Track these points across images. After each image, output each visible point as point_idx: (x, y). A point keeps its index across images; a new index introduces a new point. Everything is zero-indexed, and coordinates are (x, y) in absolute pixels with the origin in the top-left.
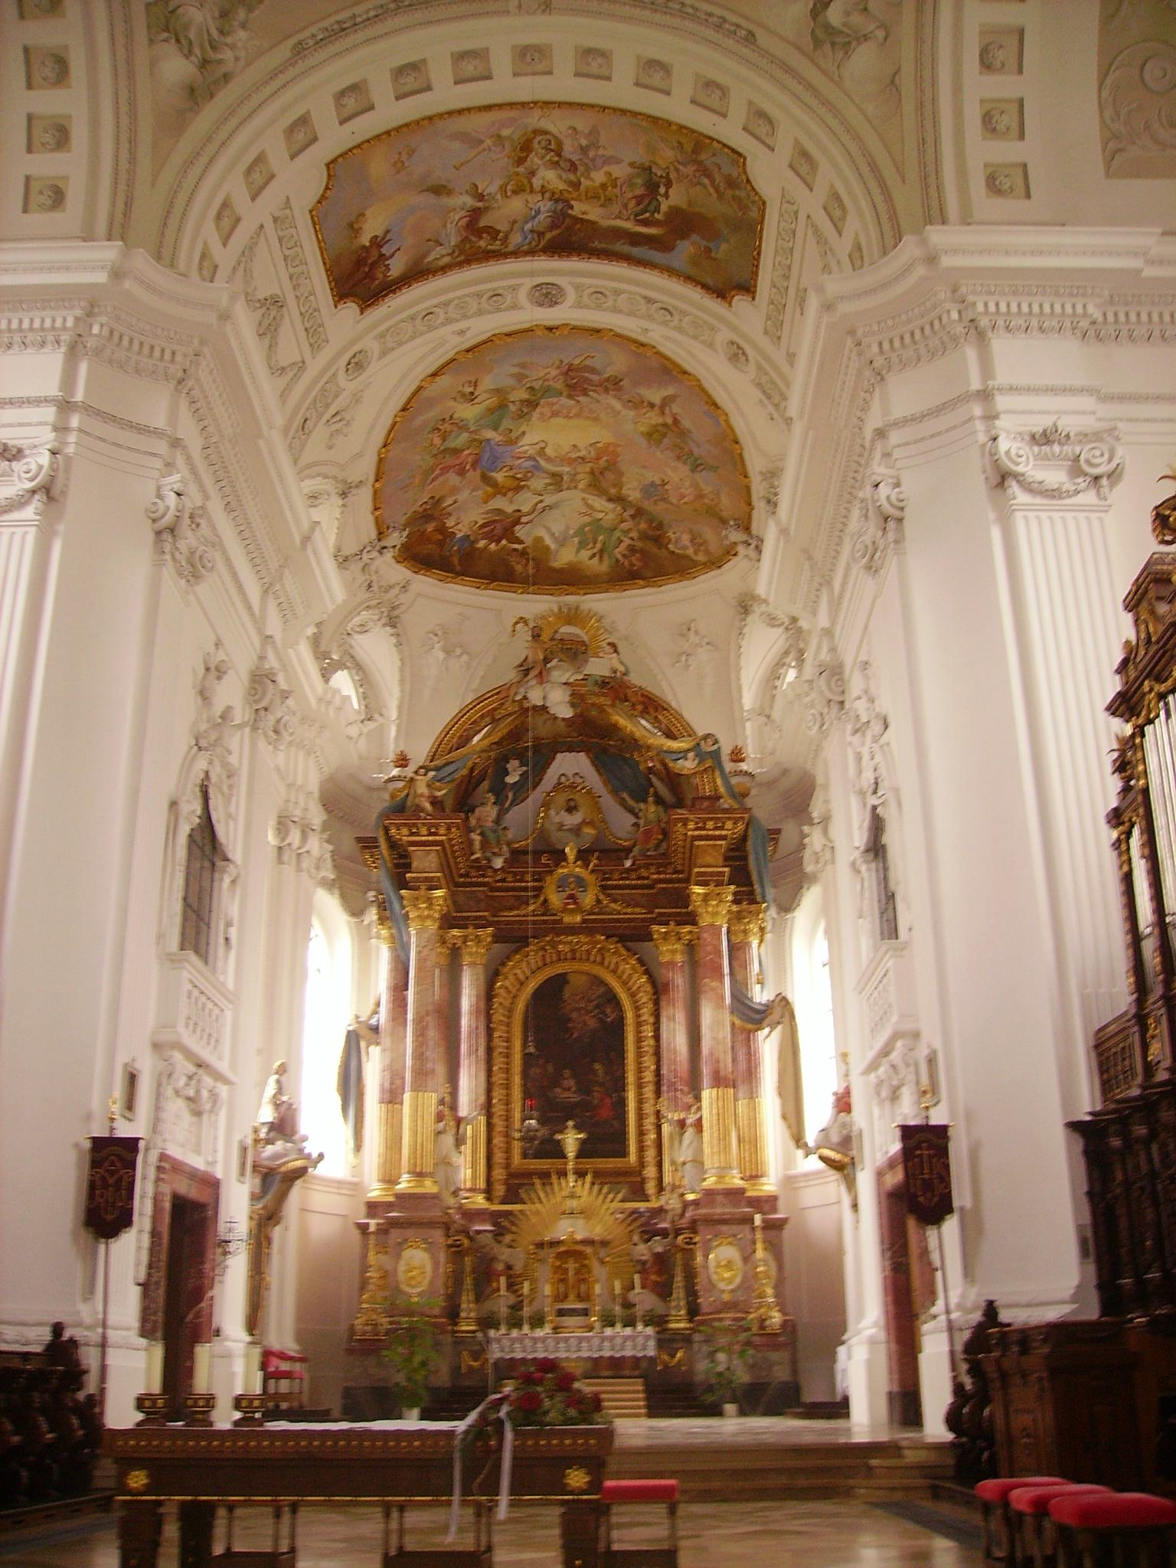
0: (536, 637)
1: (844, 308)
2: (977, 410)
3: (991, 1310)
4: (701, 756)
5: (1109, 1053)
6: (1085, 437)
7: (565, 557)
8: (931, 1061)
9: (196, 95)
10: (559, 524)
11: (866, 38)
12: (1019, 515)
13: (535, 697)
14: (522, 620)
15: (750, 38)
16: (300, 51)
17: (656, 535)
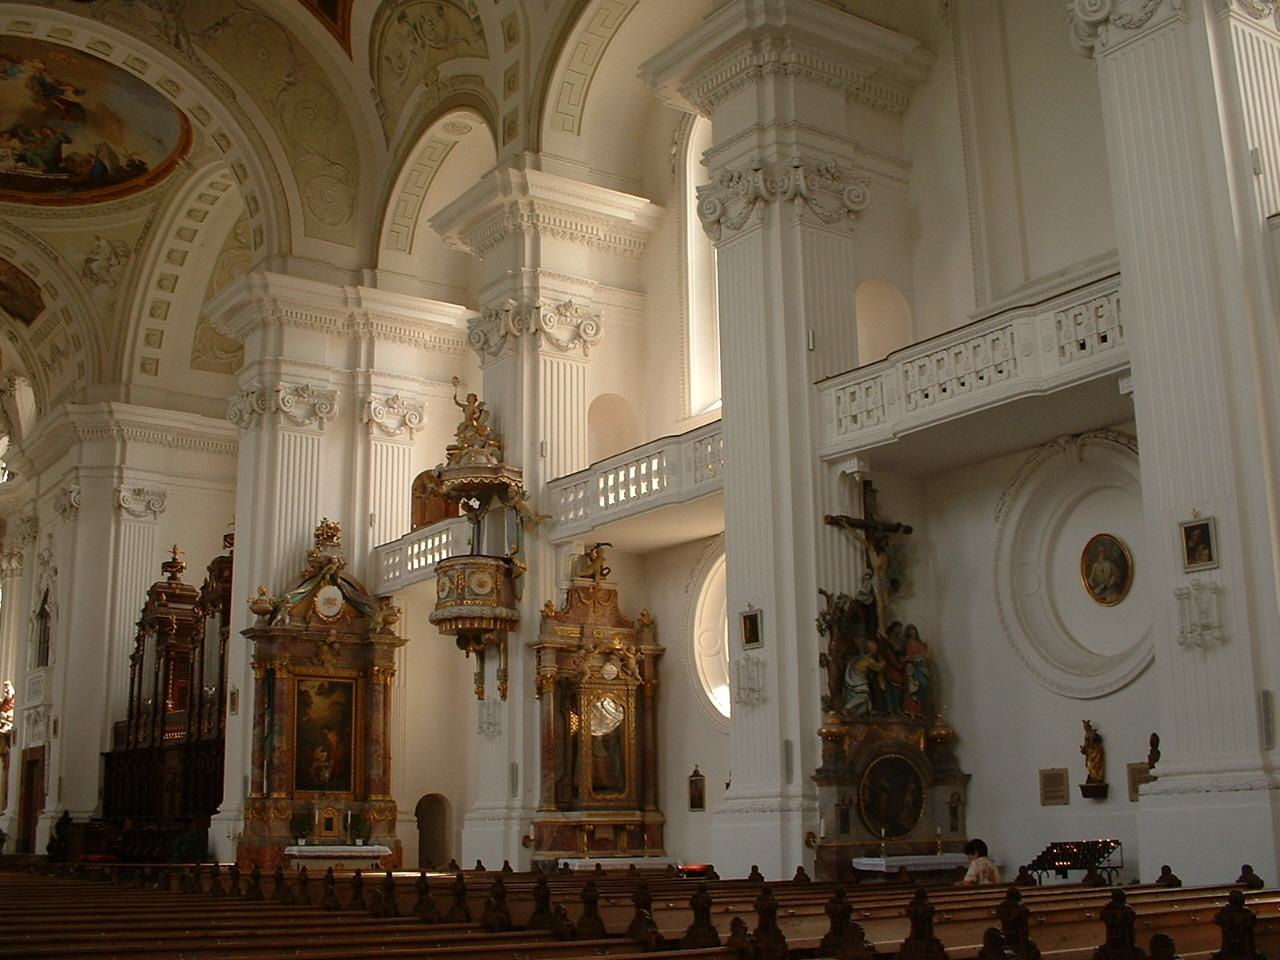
1: (72, 418)
2: (116, 474)
3: (66, 813)
5: (119, 732)
8: (55, 722)
11: (106, 282)
12: (123, 523)
15: (56, 259)
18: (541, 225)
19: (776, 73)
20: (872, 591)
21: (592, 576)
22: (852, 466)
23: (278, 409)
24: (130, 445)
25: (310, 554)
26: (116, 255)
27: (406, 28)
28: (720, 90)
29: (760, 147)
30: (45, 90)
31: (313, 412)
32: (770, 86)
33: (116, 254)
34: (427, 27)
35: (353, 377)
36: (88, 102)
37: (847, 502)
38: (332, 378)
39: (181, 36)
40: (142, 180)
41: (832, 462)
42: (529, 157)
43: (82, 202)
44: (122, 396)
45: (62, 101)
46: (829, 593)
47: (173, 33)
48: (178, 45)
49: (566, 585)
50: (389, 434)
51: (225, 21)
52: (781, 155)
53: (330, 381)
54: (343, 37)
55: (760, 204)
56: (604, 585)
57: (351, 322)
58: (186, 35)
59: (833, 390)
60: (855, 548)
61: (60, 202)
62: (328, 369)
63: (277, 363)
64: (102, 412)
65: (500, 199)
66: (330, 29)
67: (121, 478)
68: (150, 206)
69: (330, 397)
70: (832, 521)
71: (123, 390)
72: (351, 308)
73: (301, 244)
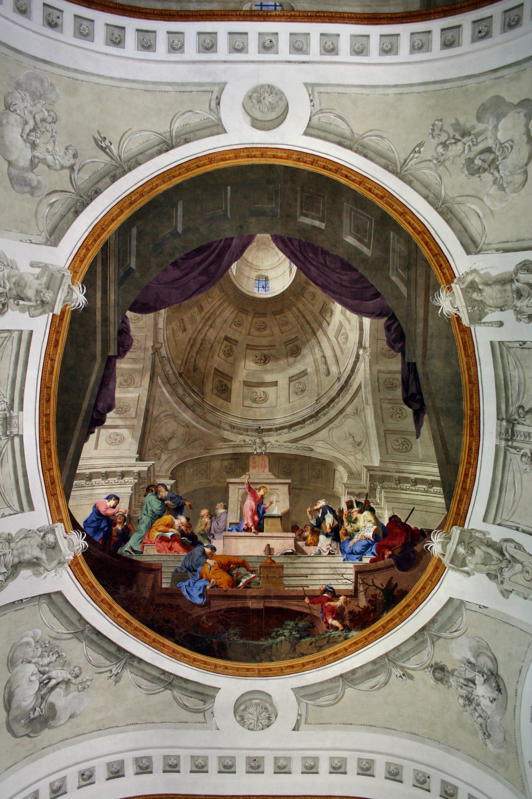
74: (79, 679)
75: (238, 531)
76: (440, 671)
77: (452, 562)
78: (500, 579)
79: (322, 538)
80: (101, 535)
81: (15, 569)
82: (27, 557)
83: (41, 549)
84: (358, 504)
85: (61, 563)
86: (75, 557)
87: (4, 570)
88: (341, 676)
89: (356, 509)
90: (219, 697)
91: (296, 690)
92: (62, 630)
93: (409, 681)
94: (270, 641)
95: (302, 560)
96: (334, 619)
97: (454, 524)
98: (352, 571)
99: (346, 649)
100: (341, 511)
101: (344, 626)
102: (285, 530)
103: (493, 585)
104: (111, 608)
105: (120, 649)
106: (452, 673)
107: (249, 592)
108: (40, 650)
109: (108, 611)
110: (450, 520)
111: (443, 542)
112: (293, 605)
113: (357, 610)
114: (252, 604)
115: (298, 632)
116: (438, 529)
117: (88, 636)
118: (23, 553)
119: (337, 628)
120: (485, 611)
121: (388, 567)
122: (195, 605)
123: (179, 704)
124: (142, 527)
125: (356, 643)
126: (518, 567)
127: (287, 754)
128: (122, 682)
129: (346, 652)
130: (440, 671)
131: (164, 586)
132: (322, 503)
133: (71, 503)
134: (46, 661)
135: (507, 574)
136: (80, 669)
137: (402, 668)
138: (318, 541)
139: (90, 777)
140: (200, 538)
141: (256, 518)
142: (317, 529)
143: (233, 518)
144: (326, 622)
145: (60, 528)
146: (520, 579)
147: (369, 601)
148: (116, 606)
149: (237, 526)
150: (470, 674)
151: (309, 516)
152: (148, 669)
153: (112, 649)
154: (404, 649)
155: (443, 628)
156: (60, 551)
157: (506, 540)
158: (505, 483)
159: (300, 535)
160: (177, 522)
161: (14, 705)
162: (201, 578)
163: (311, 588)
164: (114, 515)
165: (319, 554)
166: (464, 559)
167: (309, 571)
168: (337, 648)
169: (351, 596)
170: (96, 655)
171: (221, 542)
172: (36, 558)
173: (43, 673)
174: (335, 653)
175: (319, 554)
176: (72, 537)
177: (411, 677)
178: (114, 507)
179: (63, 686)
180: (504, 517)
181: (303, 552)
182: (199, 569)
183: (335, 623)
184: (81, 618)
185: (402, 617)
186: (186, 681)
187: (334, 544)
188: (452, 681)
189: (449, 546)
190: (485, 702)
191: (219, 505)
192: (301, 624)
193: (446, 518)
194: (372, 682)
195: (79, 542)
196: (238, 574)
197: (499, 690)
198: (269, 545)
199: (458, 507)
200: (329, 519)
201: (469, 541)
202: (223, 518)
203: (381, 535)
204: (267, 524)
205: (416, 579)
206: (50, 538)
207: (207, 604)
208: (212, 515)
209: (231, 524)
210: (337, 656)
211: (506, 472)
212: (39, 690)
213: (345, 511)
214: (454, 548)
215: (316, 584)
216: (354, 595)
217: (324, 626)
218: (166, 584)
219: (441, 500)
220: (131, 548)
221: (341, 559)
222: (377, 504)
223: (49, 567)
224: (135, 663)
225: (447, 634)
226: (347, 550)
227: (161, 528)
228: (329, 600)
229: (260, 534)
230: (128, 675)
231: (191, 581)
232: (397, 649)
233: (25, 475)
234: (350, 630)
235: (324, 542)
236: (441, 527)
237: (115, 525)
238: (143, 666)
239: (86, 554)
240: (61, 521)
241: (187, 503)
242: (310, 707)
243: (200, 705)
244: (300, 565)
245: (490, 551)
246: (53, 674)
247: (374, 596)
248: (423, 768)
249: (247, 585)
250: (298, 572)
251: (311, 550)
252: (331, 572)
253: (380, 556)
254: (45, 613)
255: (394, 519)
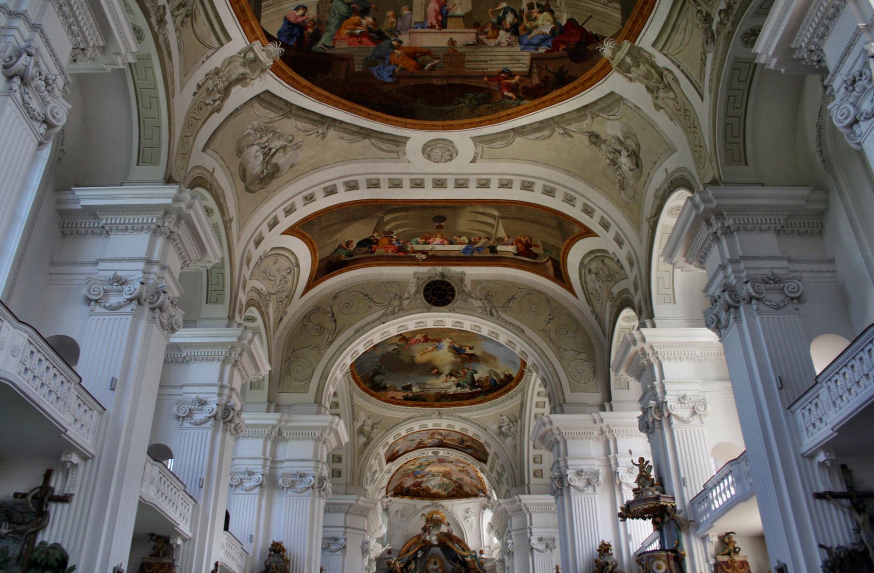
0: (427, 520)
1: (503, 506)
4: (472, 557)
6: (549, 539)
7: (435, 490)
9: (366, 445)
10: (433, 484)
13: (428, 538)
14: (423, 515)
15: (485, 430)
16: (387, 430)
17: (460, 487)
18: (660, 358)
19: (725, 234)
20: (862, 541)
21: (729, 554)
22: (821, 457)
23: (569, 485)
24: (533, 515)
25: (596, 561)
26: (511, 421)
27: (593, 275)
28: (702, 254)
29: (725, 277)
30: (457, 351)
31: (589, 483)
32: (724, 242)
33: (511, 421)
34: (601, 272)
35: (608, 460)
36: (477, 352)
37: (829, 482)
38: (597, 463)
39: (493, 311)
40: (512, 383)
41: (811, 456)
42: (648, 322)
43: (490, 400)
44: (527, 491)
45: (467, 354)
46: (829, 545)
47: (488, 309)
48: (492, 314)
49: (712, 562)
50: (581, 491)
51: (513, 298)
52: (738, 278)
53: (598, 465)
54: (571, 289)
55: (732, 310)
56: (737, 558)
57: (602, 432)
58: (495, 308)
59: (799, 411)
60: (844, 512)
61: (481, 402)
62: (594, 458)
63: (566, 461)
64: (516, 501)
65: (633, 349)
66: (564, 287)
67: (531, 533)
68: (520, 395)
69: (596, 474)
70: (819, 496)
71: (526, 488)
72: (599, 425)
73: (570, 396)
74: (293, 143)
75: (423, 28)
76: (595, 138)
77: (619, 66)
78: (655, 95)
79: (502, 32)
80: (295, 39)
81: (226, 92)
82: (234, 77)
83: (244, 66)
84: (538, 6)
85: (263, 71)
86: (275, 62)
87: (219, 95)
88: (513, 129)
89: (536, 9)
90: (409, 143)
91: (474, 139)
92: (273, 115)
93: (569, 139)
94: (452, 107)
95: (482, 49)
96: (509, 91)
97: (626, 38)
98: (528, 58)
99: (518, 112)
100: (522, 12)
101: (518, 97)
102: (467, 27)
103: (649, 97)
104: (311, 90)
105: (323, 117)
106: (604, 141)
107: (433, 73)
108: (259, 135)
109: (309, 93)
110: (624, 33)
111: (613, 49)
112: (474, 83)
113: (530, 86)
114: (435, 82)
115: (477, 100)
116: (611, 37)
117: (295, 114)
118: (230, 76)
119: (511, 98)
120: (639, 111)
121: (561, 58)
122: (385, 83)
123: (376, 147)
124: (332, 28)
125: (527, 108)
126: (671, 94)
127: (465, 177)
128: (328, 138)
129: (518, 114)
130: (595, 138)
131: (356, 70)
132: (504, 5)
133: (263, 21)
134: (265, 139)
135: (662, 94)
136: (293, 136)
137: (564, 129)
138: (498, 35)
139: (311, 198)
140: (387, 34)
141: (440, 18)
142: (498, 25)
143: (417, 17)
144: (502, 94)
145: (257, 45)
146: (671, 103)
147: (542, 80)
148: (316, 88)
149: (422, 25)
150: (618, 147)
151: (491, 16)
152: (348, 127)
153: (317, 118)
154: (568, 117)
155: (602, 110)
156: (261, 61)
157: (667, 70)
158: (678, 25)
159: (481, 31)
160: (364, 22)
161: (248, 175)
162: (390, 63)
163: (489, 70)
164: (304, 21)
165: (499, 45)
166: (630, 68)
167: (488, 58)
168: (510, 111)
169: (525, 76)
170: (304, 124)
171: (407, 36)
172: (242, 74)
173: (264, 148)
174: (508, 115)
175: (499, 45)
176: (269, 48)
177: (571, 136)
178: (303, 15)
179: (282, 151)
180: (670, 51)
181: (484, 44)
182: (388, 57)
183: (510, 94)
184: (287, 103)
185: (569, 95)
186: (381, 133)
187: (513, 38)
188: (603, 146)
189: (619, 54)
190: (625, 169)
191: (404, 7)
192: (480, 95)
193: (619, 32)
194: (539, 134)
195: (275, 49)
196: (423, 61)
197: (637, 165)
198: (451, 39)
199: (632, 26)
200: (510, 18)
201: (637, 56)
202: (408, 17)
203: (558, 32)
204: (450, 22)
205: (585, 70)
206: (251, 55)
207: (397, 82)
208: (398, 16)
209: (415, 23)
210: (509, 117)
211: (681, 17)
212: (264, 159)
213: (526, 11)
214: (623, 56)
215: (495, 67)
216: (530, 74)
217: (500, 97)
218: (358, 68)
219: (618, 16)
220: (324, 45)
221: (519, 49)
222: (557, 7)
223: (254, 77)
224: (337, 124)
225: (605, 115)
226: (525, 41)
227: (350, 27)
228: (505, 78)
229: (444, 30)
230: (332, 133)
231: (381, 67)
232: (562, 116)
233: (217, 16)
234: (522, 100)
235: (503, 36)
236: (614, 37)
237: (306, 29)
238: (343, 126)
239: (283, 57)
240: (257, 39)
241: (373, 6)
242: (485, 149)
243: (395, 148)
244: (481, 54)
245: (653, 71)
246: (272, 145)
247: (546, 77)
248: (572, 193)
249: (433, 68)
250: (478, 58)
251: (492, 42)
252: (509, 58)
253: (555, 47)
254: (258, 109)
255: (571, 22)
